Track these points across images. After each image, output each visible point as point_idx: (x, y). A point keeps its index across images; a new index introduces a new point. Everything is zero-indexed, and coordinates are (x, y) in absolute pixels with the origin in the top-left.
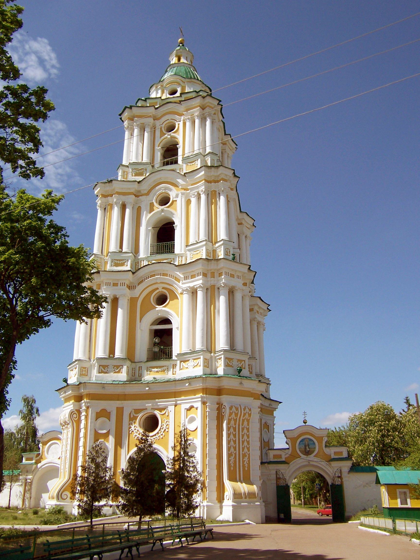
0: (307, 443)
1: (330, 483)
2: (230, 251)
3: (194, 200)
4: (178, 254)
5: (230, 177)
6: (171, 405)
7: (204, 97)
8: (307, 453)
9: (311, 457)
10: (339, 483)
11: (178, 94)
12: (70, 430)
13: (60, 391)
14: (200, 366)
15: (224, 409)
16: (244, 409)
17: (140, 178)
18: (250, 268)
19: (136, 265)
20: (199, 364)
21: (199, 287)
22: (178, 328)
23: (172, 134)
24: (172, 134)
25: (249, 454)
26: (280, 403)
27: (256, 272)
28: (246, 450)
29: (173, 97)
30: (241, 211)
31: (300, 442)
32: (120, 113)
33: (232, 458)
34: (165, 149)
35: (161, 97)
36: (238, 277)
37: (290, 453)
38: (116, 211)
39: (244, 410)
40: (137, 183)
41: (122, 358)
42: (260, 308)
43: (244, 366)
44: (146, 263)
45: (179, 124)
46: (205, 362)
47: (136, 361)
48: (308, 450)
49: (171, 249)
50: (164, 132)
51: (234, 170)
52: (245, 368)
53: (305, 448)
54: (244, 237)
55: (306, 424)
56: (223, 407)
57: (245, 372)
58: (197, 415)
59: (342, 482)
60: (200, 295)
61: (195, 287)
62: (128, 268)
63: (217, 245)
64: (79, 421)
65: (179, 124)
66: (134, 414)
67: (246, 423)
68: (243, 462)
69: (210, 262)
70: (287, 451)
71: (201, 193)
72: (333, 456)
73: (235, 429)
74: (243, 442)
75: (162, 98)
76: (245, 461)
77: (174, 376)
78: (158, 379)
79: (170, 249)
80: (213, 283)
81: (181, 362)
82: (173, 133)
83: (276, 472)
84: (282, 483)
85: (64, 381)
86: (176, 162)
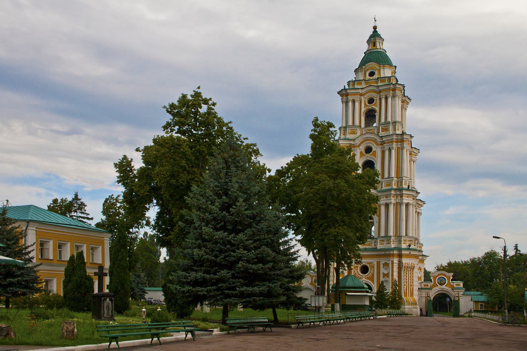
1: (453, 299)
6: (375, 261)
8: (441, 284)
9: (444, 286)
10: (457, 299)
16: (411, 264)
23: (372, 106)
24: (372, 106)
25: (413, 285)
28: (412, 283)
33: (405, 287)
36: (411, 197)
37: (432, 284)
42: (419, 204)
45: (376, 99)
50: (367, 104)
53: (441, 282)
57: (412, 247)
59: (459, 299)
65: (376, 99)
67: (412, 270)
68: (410, 288)
74: (410, 279)
82: (373, 105)
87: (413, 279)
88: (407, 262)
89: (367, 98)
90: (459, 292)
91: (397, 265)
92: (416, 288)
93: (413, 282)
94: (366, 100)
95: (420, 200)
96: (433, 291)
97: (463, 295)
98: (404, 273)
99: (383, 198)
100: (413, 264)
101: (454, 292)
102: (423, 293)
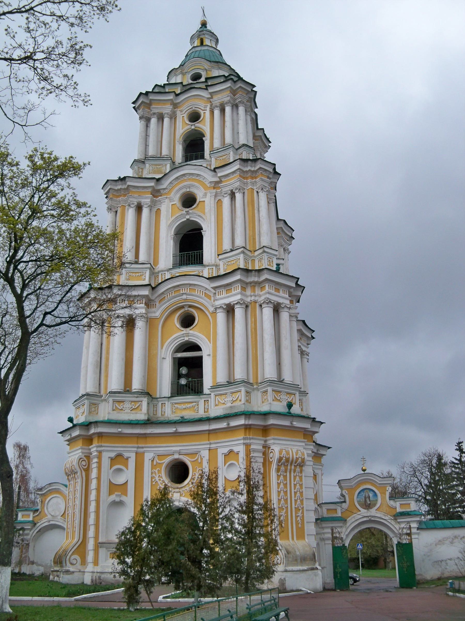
0: (367, 495)
2: (272, 261)
3: (226, 201)
4: (208, 266)
5: (271, 172)
6: (204, 449)
7: (235, 82)
8: (368, 506)
9: (373, 512)
11: (203, 79)
12: (79, 480)
13: (64, 434)
14: (240, 401)
15: (272, 454)
16: (297, 454)
17: (158, 176)
18: (297, 281)
19: (155, 278)
20: (240, 397)
21: (236, 304)
22: (209, 355)
24: (197, 125)
25: (303, 508)
26: (329, 448)
27: (304, 287)
29: (197, 83)
30: (278, 219)
31: (359, 493)
32: (135, 99)
34: (188, 142)
35: (182, 83)
38: (131, 214)
39: (296, 455)
40: (155, 180)
41: (142, 392)
43: (294, 401)
44: (168, 276)
46: (246, 396)
47: (158, 396)
48: (369, 503)
49: (199, 260)
50: (188, 122)
51: (274, 165)
52: (295, 404)
53: (365, 501)
54: (282, 249)
55: (365, 472)
56: (270, 451)
57: (296, 409)
58: (238, 461)
60: (239, 312)
61: (232, 303)
62: (147, 282)
63: (257, 253)
64: (87, 470)
66: (158, 461)
67: (298, 469)
68: (297, 517)
69: (250, 274)
70: (344, 504)
71: (236, 192)
72: (399, 510)
73: (285, 477)
74: (295, 493)
75: (184, 84)
76: (298, 516)
77: (206, 414)
78: (185, 417)
79: (197, 260)
80: (253, 298)
81: (216, 396)
83: (332, 530)
84: (338, 543)
85: (69, 421)
86: (202, 157)
87: (301, 493)
88: (283, 447)
89: (187, 112)
90: (408, 522)
91: (261, 455)
92: (311, 517)
93: (302, 501)
94: (186, 116)
95: (304, 322)
96: (348, 524)
97: (418, 529)
98: (278, 476)
99: (220, 293)
100: (300, 453)
101: (399, 523)
102: (326, 530)
